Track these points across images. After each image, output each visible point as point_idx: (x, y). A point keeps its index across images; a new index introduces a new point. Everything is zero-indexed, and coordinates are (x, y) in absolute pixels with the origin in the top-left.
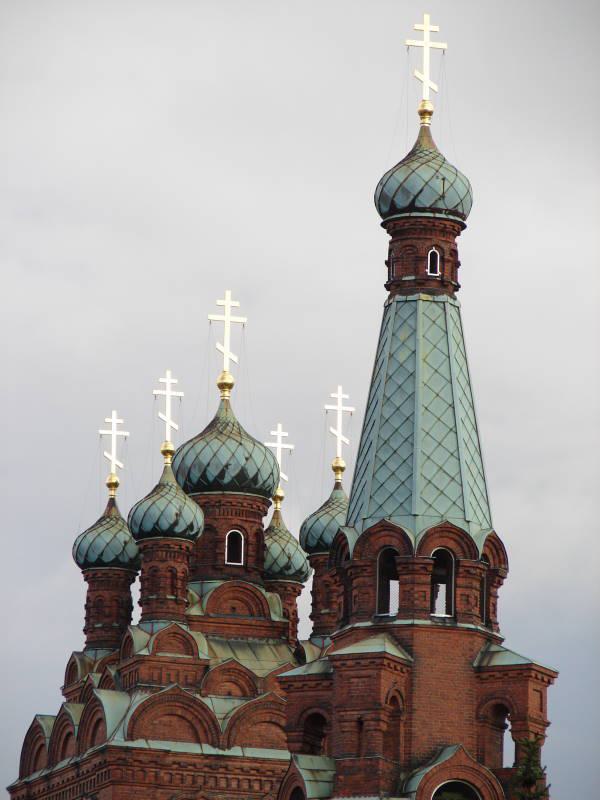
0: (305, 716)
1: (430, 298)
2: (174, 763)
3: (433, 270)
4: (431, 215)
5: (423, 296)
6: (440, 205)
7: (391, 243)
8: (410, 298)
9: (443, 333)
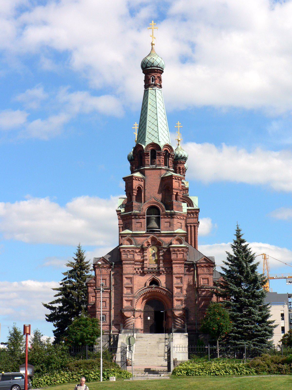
1: (152, 89)
3: (153, 81)
4: (151, 68)
5: (150, 88)
6: (152, 65)
7: (145, 76)
9: (155, 97)
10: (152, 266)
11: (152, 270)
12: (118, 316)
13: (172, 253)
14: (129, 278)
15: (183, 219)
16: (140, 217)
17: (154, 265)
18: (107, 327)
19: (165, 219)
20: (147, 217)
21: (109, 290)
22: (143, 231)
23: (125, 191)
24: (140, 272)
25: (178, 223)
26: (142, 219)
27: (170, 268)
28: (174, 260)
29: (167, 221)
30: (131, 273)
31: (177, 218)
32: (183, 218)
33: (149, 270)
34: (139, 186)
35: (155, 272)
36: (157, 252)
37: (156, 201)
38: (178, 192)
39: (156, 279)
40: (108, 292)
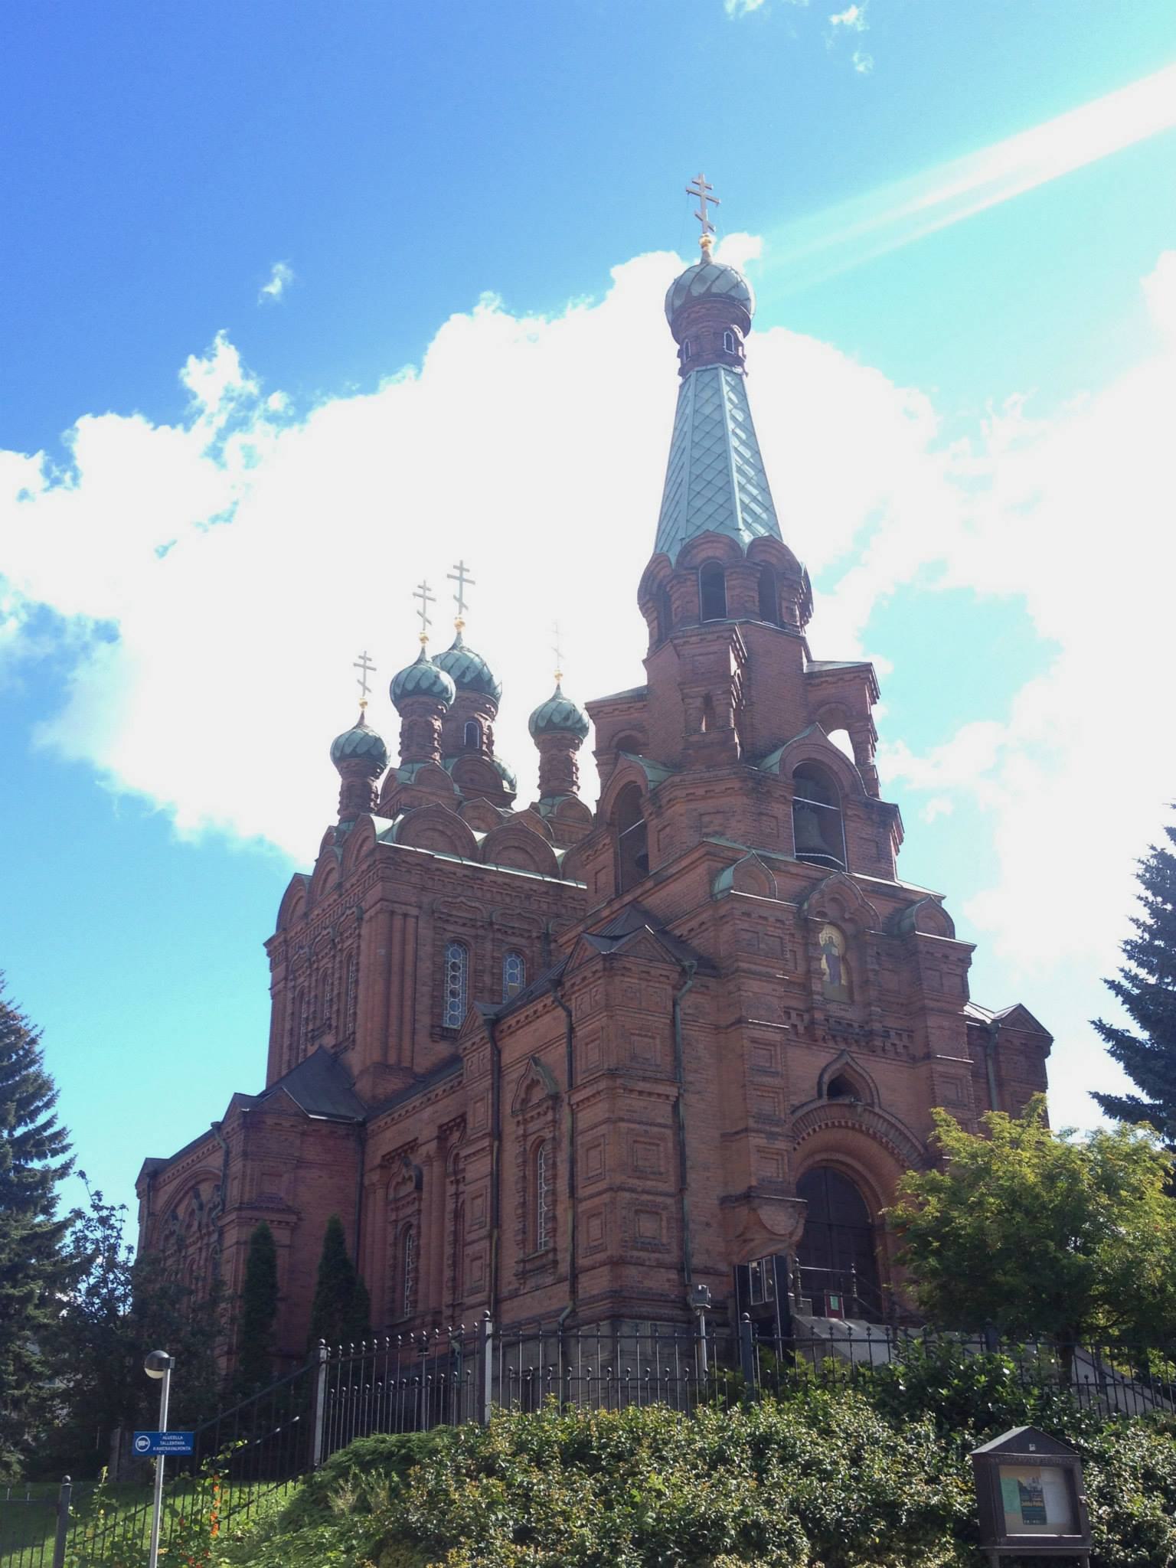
0: (616, 739)
2: (438, 869)
8: (709, 367)
10: (834, 1009)
12: (708, 1225)
14: (766, 1044)
18: (669, 1280)
21: (672, 1091)
24: (794, 1026)
27: (905, 1031)
28: (931, 999)
39: (858, 1069)
40: (667, 1097)
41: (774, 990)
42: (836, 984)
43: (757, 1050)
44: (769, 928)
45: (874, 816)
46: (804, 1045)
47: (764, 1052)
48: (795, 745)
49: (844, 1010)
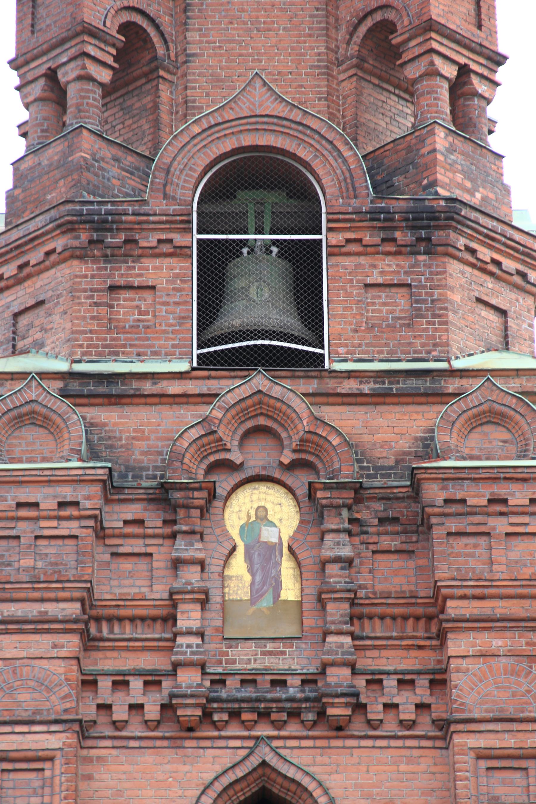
11: (248, 692)
13: (437, 531)
15: (517, 279)
16: (143, 243)
17: (270, 647)
19: (362, 260)
20: (198, 241)
22: (169, 356)
23: (14, 64)
25: (479, 300)
26: (157, 262)
28: (464, 597)
29: (380, 280)
30: (53, 717)
31: (468, 257)
32: (519, 273)
33: (224, 694)
34: (138, 19)
35: (281, 710)
36: (292, 538)
37: (281, 110)
38: (474, 66)
39: (291, 773)
41: (55, 646)
42: (266, 602)
43: (12, 776)
44: (43, 523)
45: (398, 235)
46: (165, 743)
47: (32, 775)
48: (196, 129)
49: (270, 653)
